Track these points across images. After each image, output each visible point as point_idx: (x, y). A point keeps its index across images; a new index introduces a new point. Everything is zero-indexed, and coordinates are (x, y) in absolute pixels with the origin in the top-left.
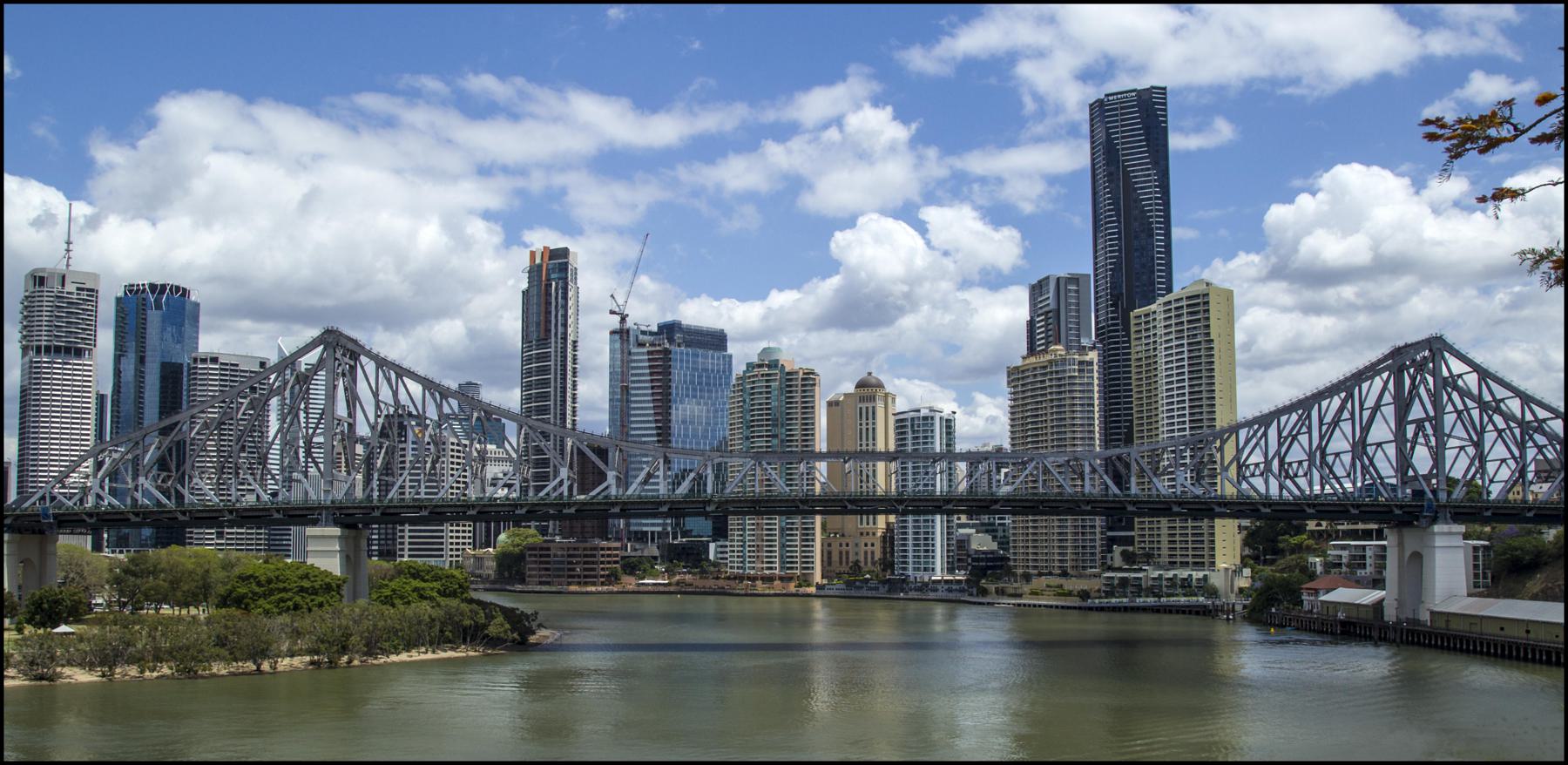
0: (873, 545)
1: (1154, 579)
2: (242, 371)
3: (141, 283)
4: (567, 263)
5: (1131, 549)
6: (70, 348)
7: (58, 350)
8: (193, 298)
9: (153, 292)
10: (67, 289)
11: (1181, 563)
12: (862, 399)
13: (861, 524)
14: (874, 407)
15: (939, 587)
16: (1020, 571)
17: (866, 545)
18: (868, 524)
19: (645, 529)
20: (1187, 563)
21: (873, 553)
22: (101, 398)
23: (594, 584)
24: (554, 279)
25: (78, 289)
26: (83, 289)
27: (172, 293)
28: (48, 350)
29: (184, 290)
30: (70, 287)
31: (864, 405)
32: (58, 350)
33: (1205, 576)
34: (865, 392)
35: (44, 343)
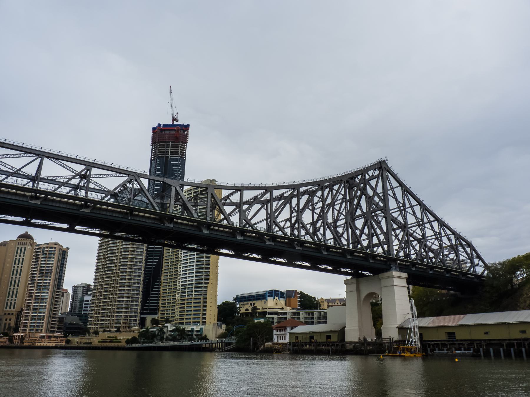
0: (10, 320)
1: (170, 331)
5: (156, 317)
11: (186, 322)
12: (19, 244)
13: (6, 308)
14: (25, 248)
15: (43, 340)
16: (92, 331)
17: (6, 320)
18: (10, 308)
20: (190, 322)
21: (9, 324)
31: (20, 247)
33: (201, 329)
34: (22, 240)
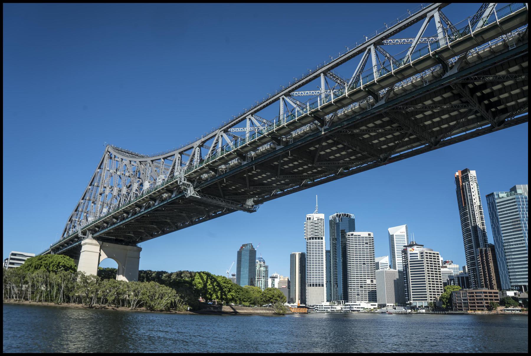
2: (362, 237)
3: (334, 215)
4: (468, 174)
6: (316, 237)
7: (313, 238)
8: (352, 217)
9: (337, 217)
10: (314, 220)
19: (519, 284)
22: (328, 252)
23: (483, 310)
24: (464, 182)
25: (318, 219)
26: (319, 219)
27: (343, 216)
28: (310, 239)
29: (348, 215)
30: (315, 219)
32: (313, 238)
35: (309, 237)
